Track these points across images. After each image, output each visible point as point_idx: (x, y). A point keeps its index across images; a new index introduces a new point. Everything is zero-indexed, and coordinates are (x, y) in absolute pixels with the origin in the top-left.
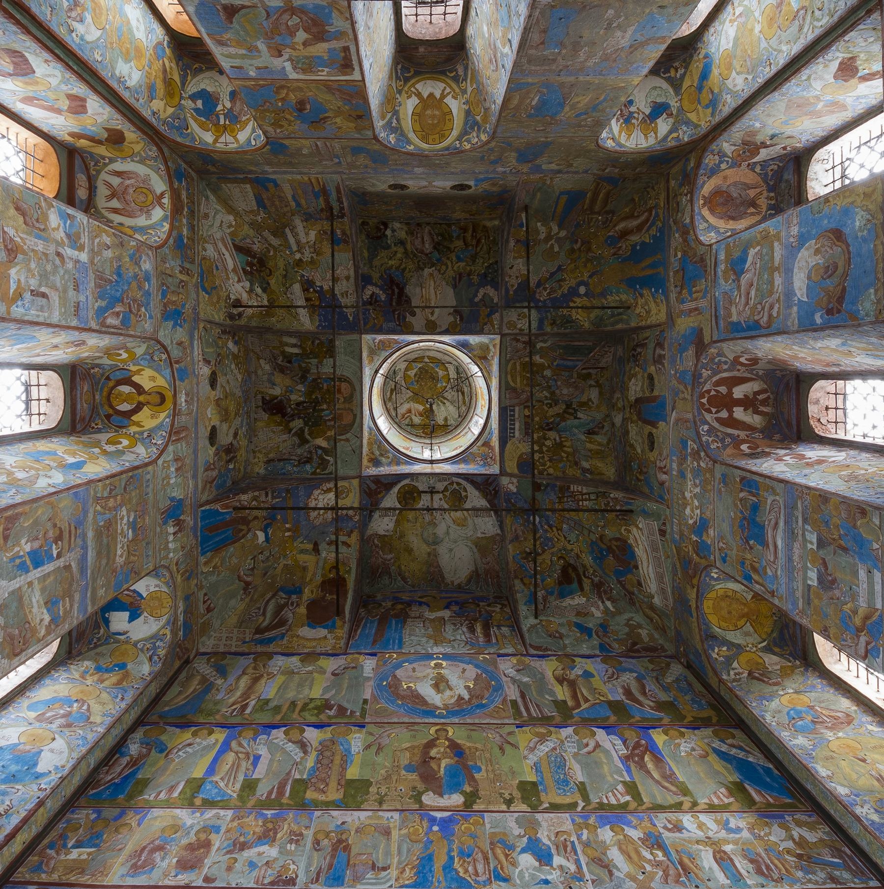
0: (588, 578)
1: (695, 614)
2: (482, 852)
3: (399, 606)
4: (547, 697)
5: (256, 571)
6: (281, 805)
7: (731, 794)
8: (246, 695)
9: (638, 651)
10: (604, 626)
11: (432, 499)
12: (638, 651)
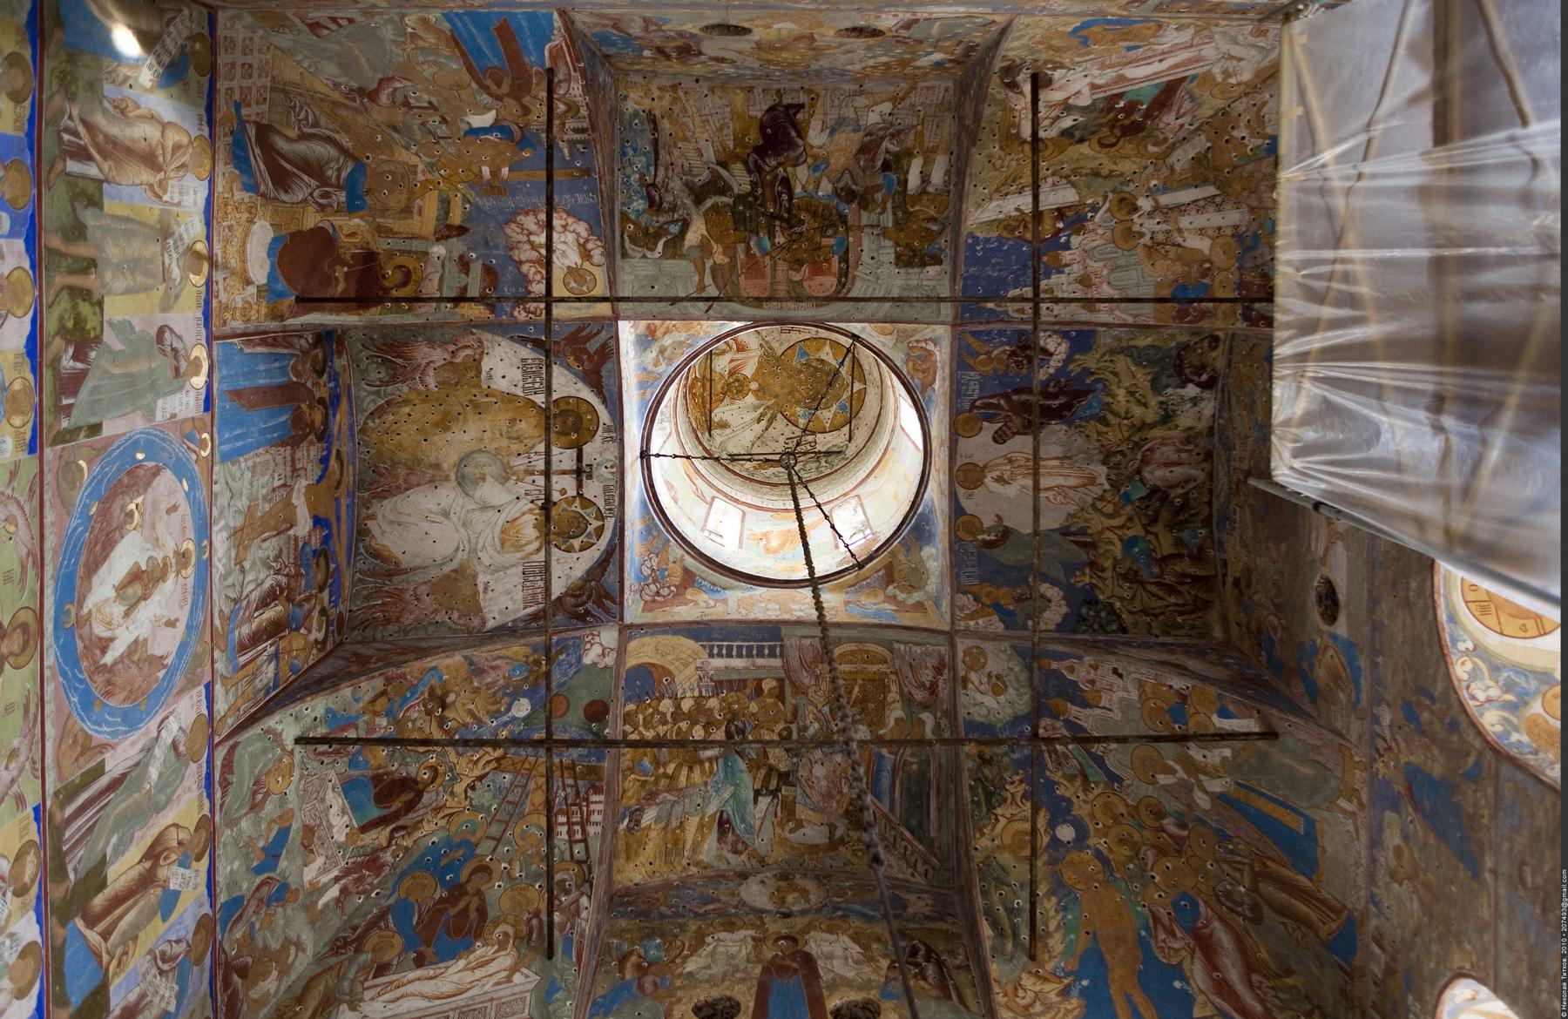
0: (391, 838)
10: (282, 893)
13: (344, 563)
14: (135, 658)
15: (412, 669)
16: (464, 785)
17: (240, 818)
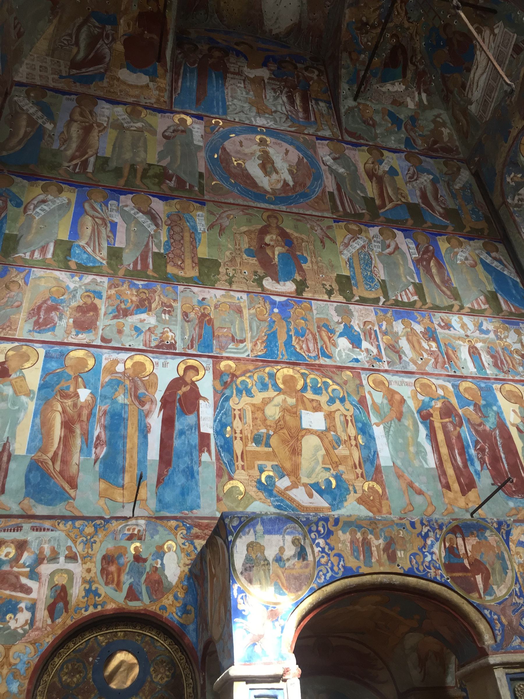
0: (414, 64)
2: (312, 333)
3: (217, 54)
4: (359, 192)
6: (148, 277)
7: (487, 301)
9: (436, 151)
10: (413, 119)
12: (436, 151)
14: (295, 171)
16: (406, 22)
17: (376, 133)
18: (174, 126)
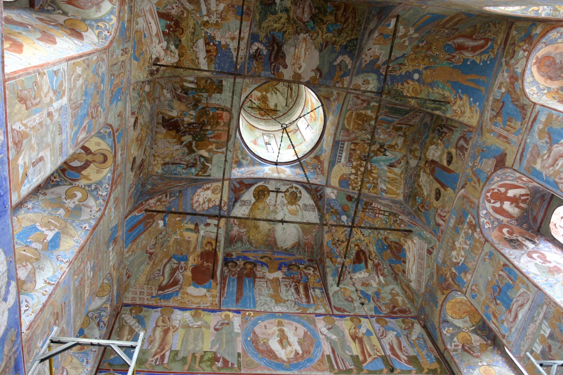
0: (371, 260)
1: (439, 308)
3: (249, 266)
4: (347, 352)
5: (157, 245)
8: (162, 346)
9: (395, 313)
10: (377, 293)
11: (277, 196)
13: (293, 257)
15: (326, 249)
16: (362, 237)
18: (221, 320)
